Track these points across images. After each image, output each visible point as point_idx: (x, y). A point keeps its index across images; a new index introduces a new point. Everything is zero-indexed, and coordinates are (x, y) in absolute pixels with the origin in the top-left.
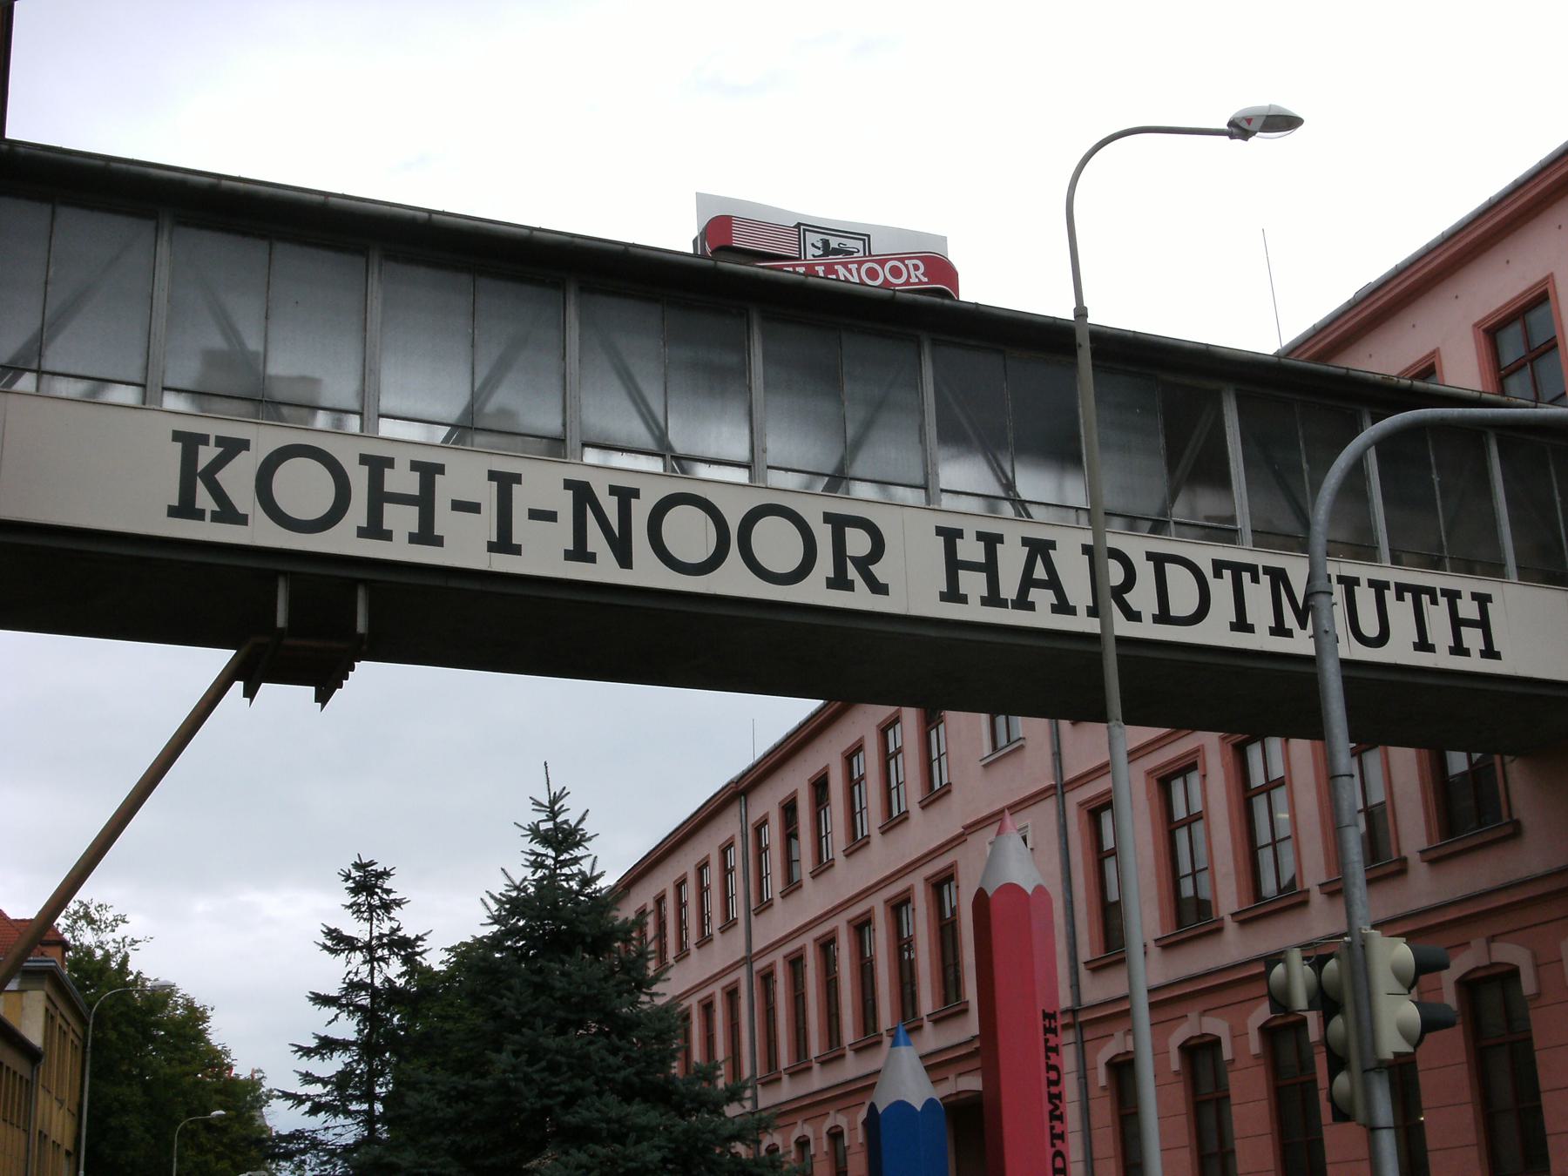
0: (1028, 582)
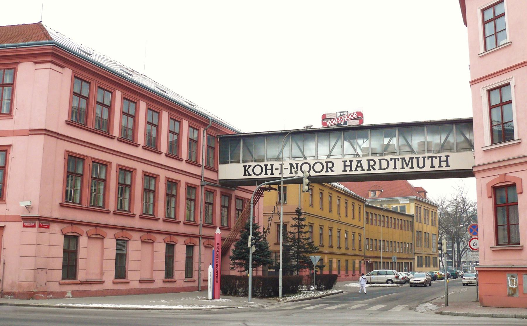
0: (357, 167)
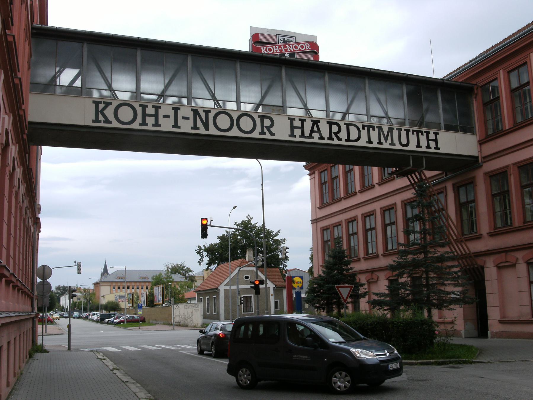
0: (312, 131)
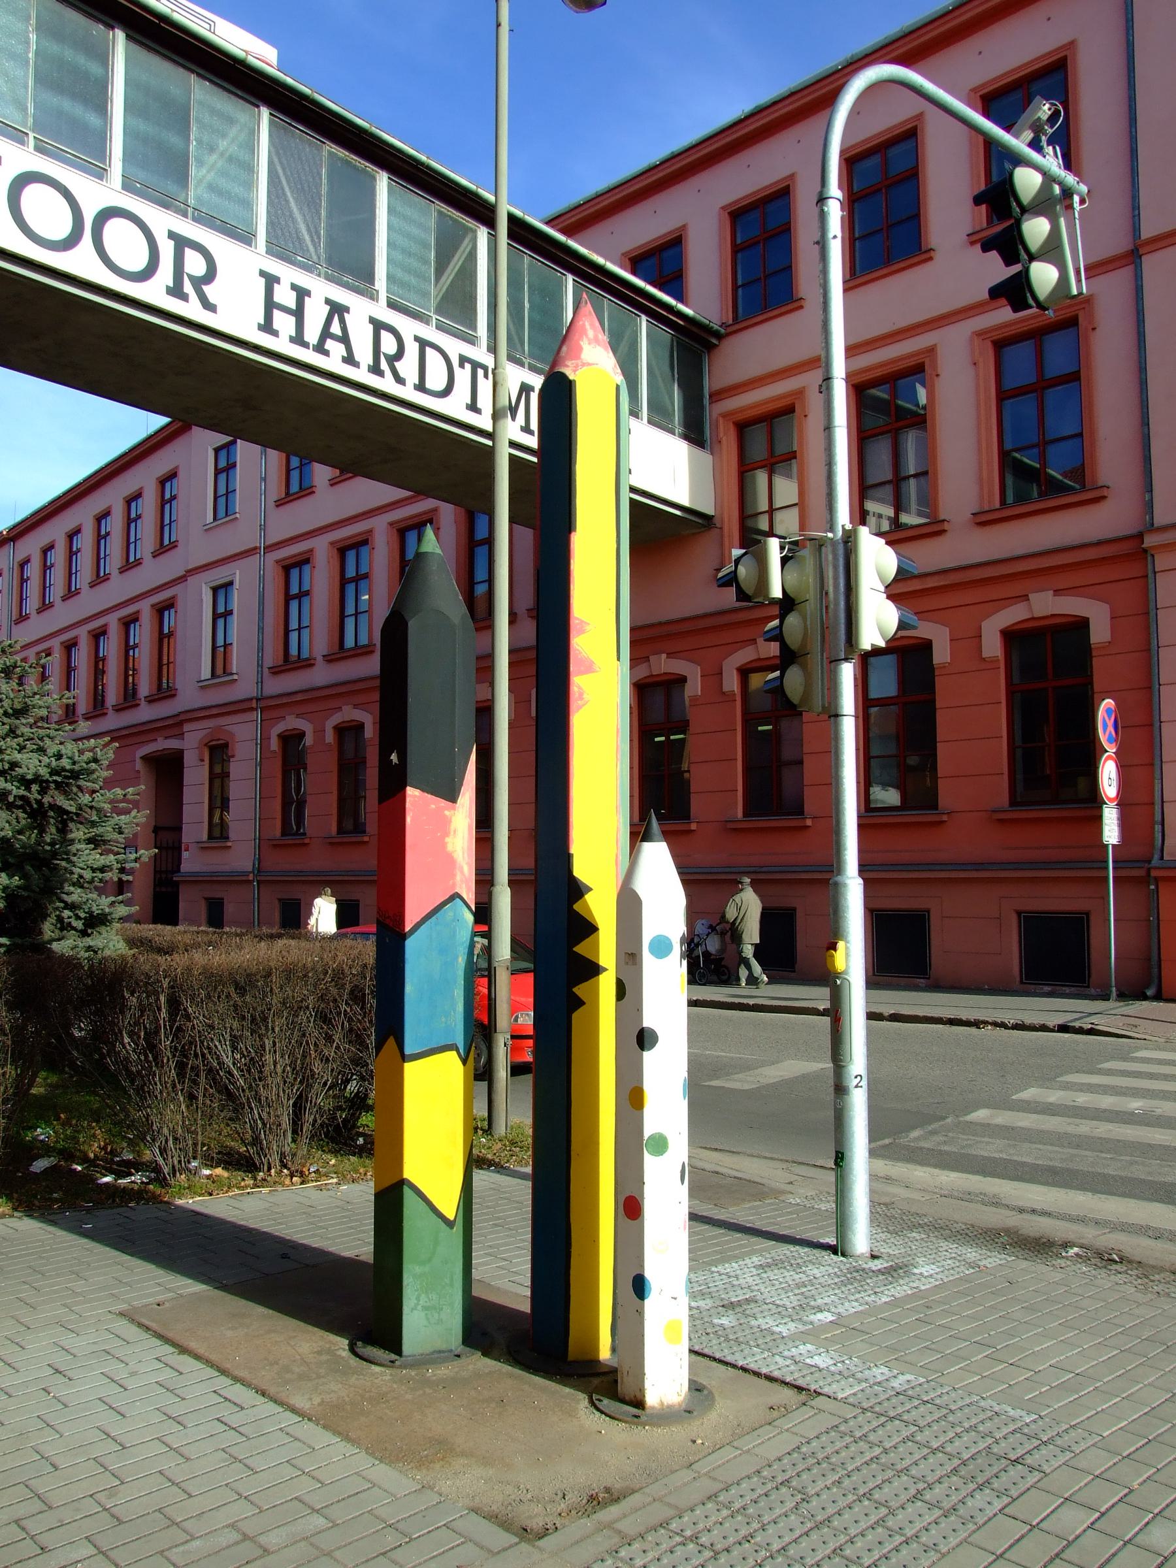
0: (326, 334)
